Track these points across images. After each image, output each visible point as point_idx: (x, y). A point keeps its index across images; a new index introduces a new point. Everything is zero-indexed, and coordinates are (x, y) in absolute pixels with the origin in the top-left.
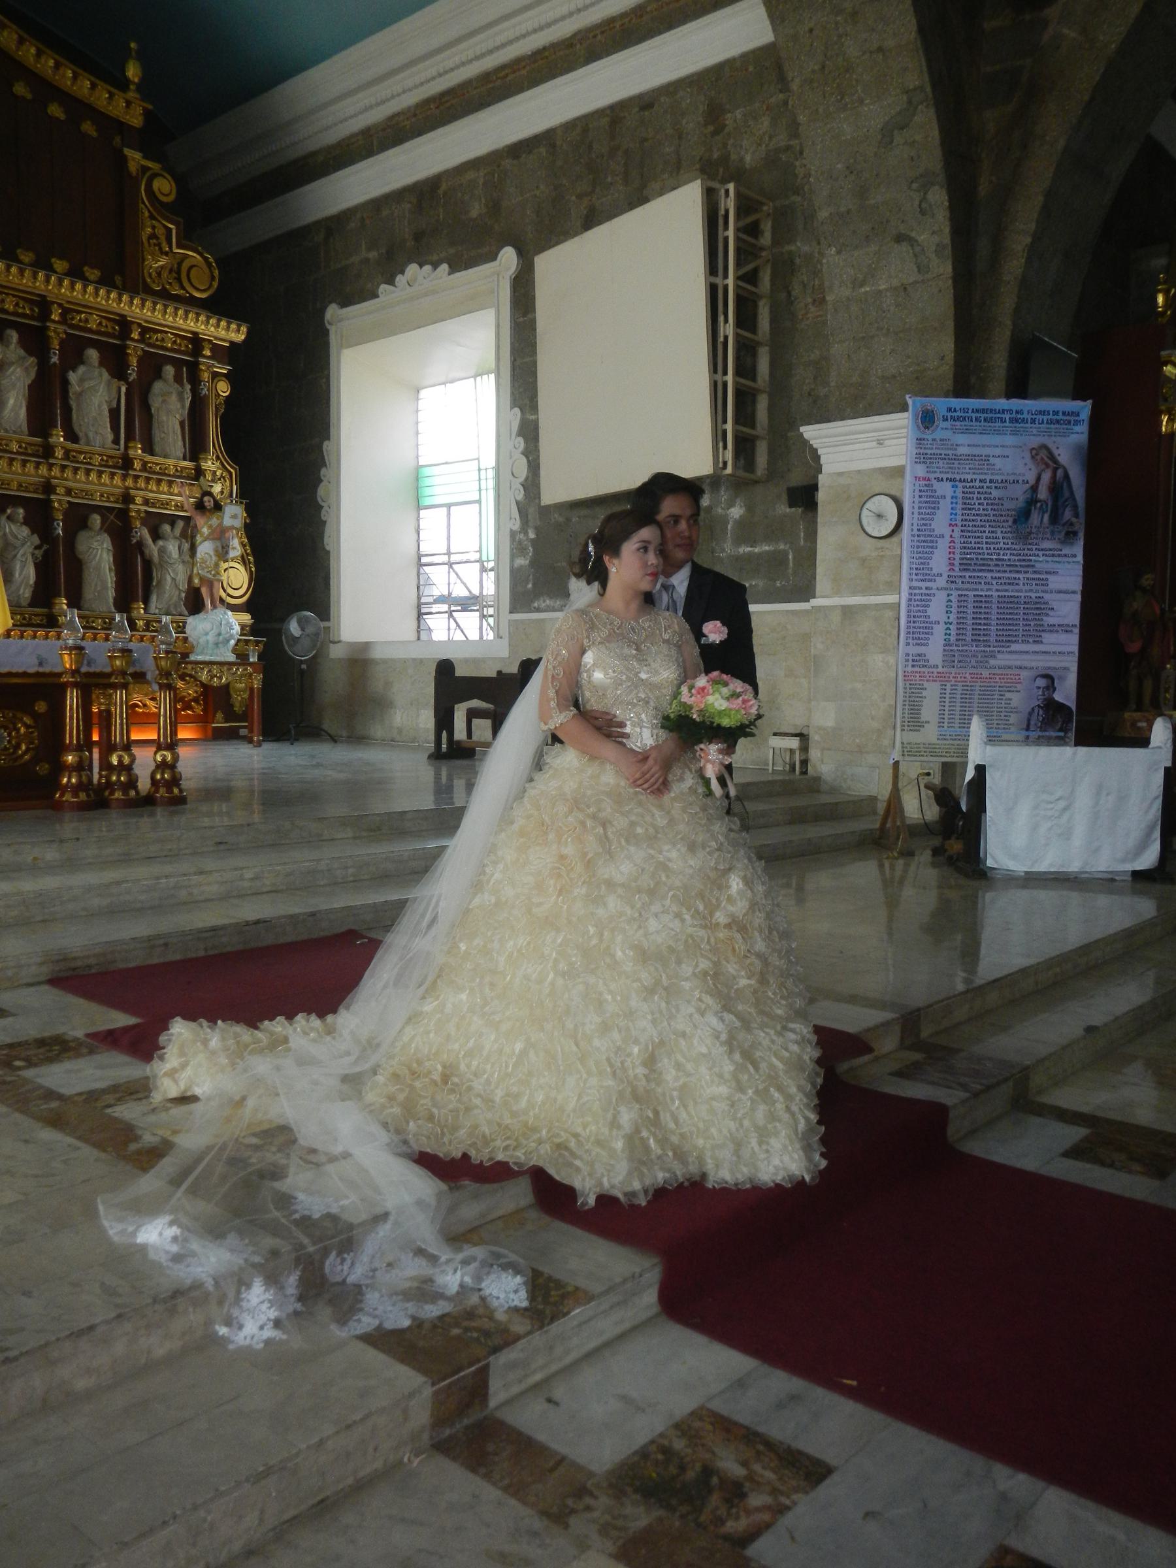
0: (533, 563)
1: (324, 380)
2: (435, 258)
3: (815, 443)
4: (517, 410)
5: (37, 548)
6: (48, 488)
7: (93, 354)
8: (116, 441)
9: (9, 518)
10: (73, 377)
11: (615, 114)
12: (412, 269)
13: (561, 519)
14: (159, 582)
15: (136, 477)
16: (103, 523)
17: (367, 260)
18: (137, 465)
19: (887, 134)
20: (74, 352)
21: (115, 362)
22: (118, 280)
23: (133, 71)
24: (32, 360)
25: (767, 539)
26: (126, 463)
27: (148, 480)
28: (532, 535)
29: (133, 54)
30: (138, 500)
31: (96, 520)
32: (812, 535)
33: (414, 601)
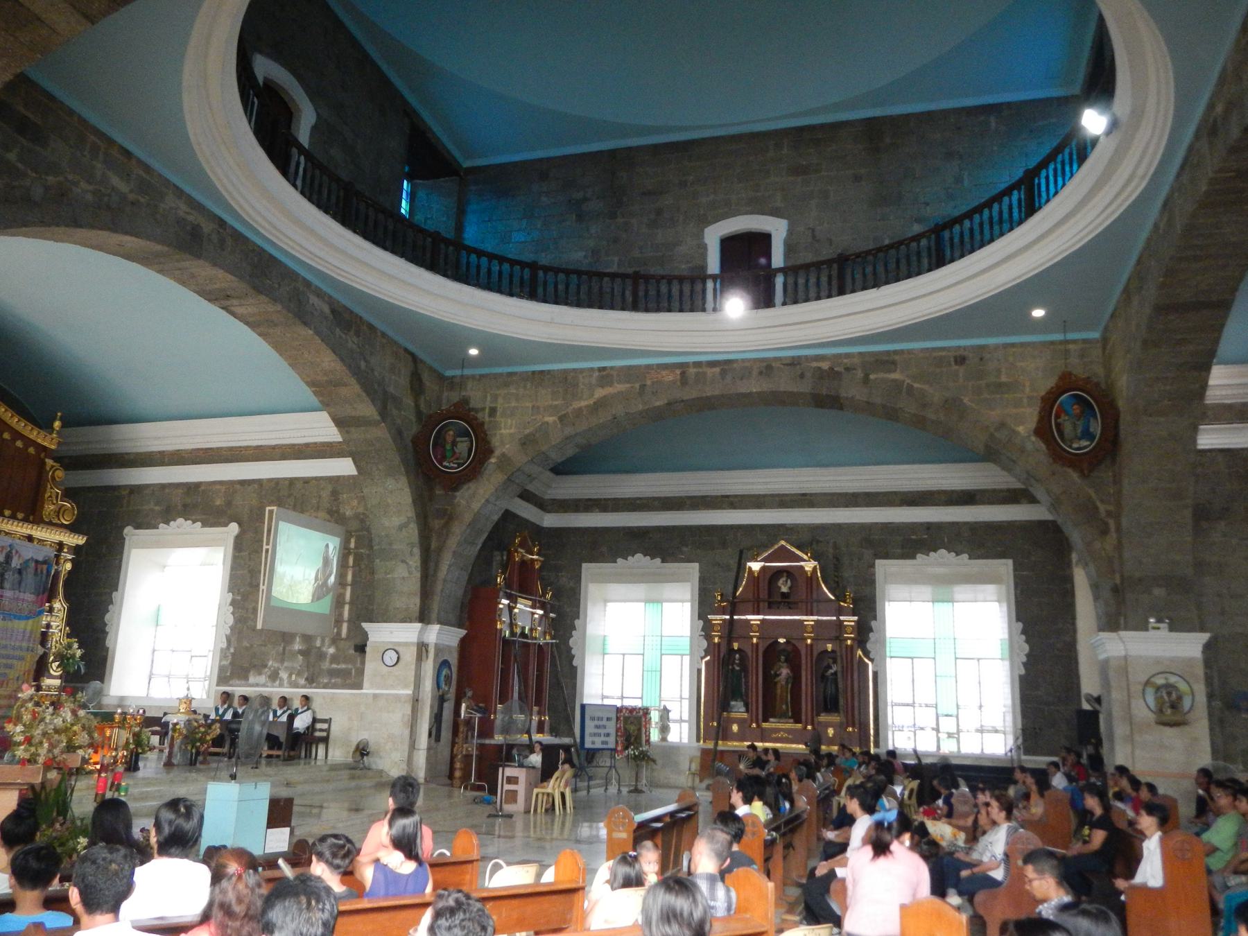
0: (230, 663)
1: (117, 561)
2: (194, 517)
3: (366, 629)
4: (231, 594)
11: (292, 482)
12: (180, 520)
13: (248, 645)
17: (152, 510)
19: (401, 528)
22: (31, 518)
23: (57, 424)
25: (344, 662)
28: (232, 650)
32: (363, 663)
33: (148, 673)
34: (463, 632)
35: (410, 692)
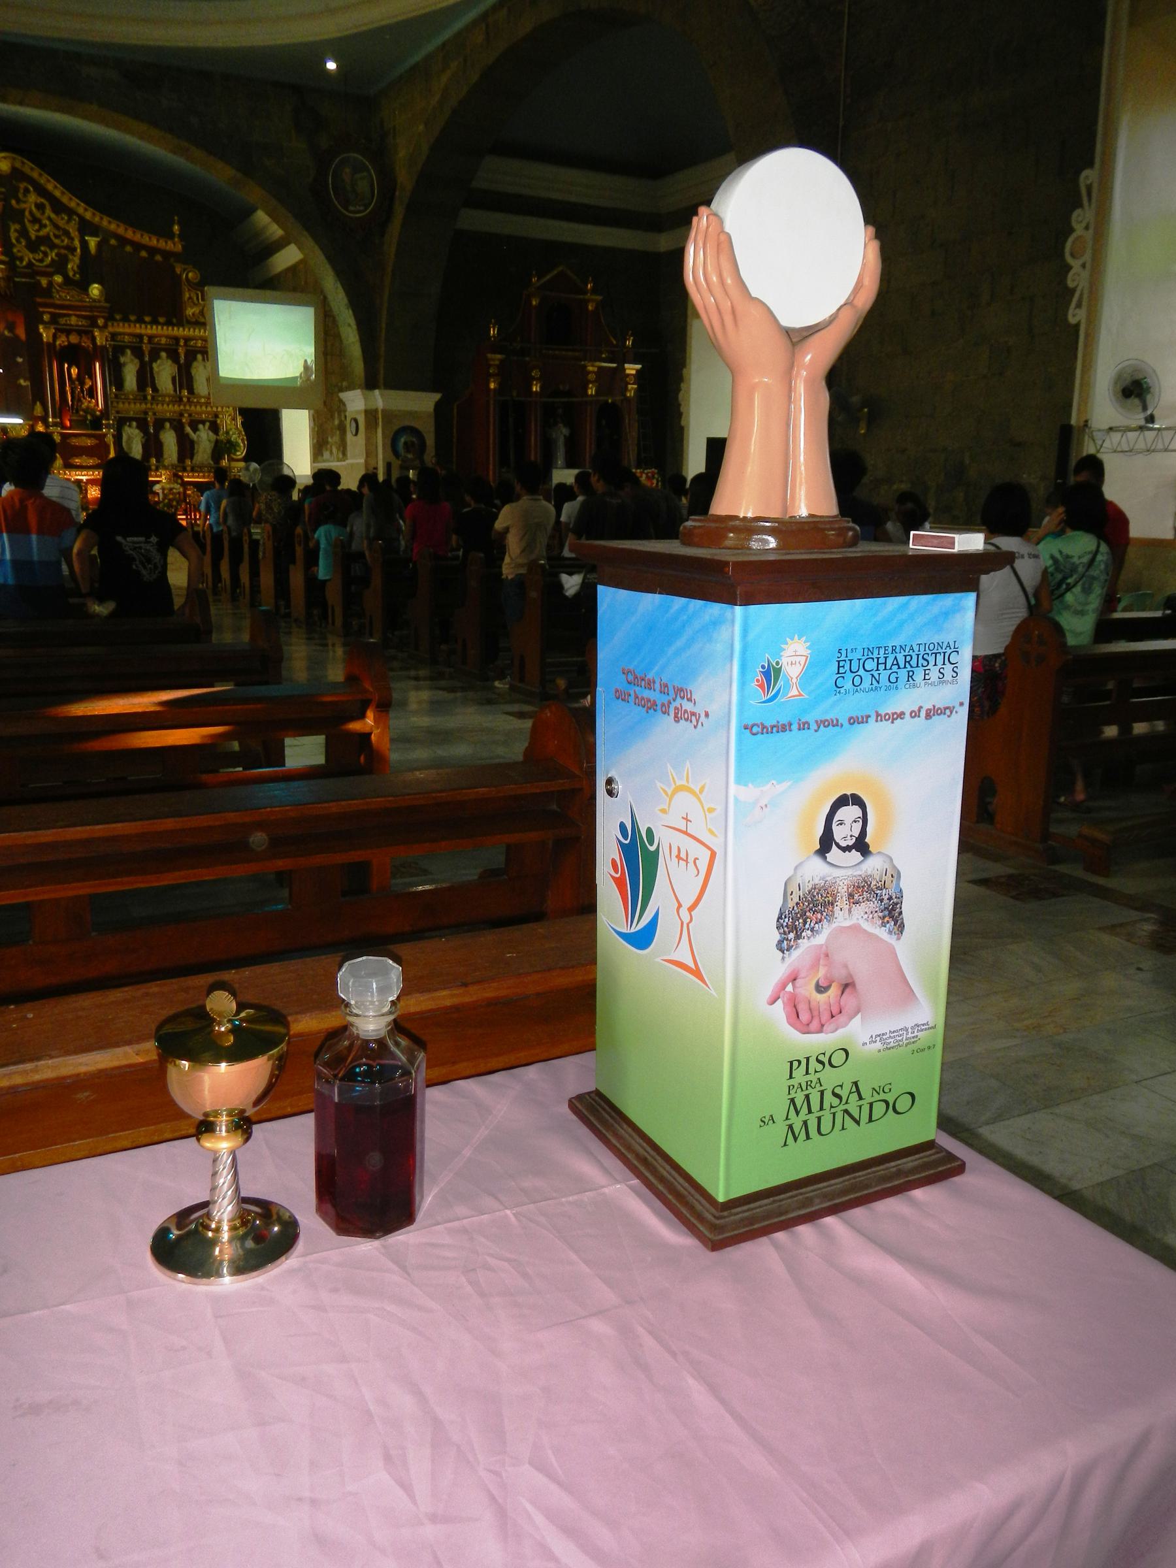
5: (143, 437)
6: (146, 413)
7: (163, 354)
8: (175, 390)
9: (130, 426)
10: (155, 365)
14: (198, 451)
15: (185, 406)
16: (171, 425)
18: (185, 399)
20: (155, 356)
21: (173, 355)
22: (174, 320)
24: (137, 361)
26: (181, 399)
27: (190, 406)
28: (316, 429)
29: (176, 221)
30: (186, 415)
31: (167, 425)
34: (437, 396)
35: (362, 461)
